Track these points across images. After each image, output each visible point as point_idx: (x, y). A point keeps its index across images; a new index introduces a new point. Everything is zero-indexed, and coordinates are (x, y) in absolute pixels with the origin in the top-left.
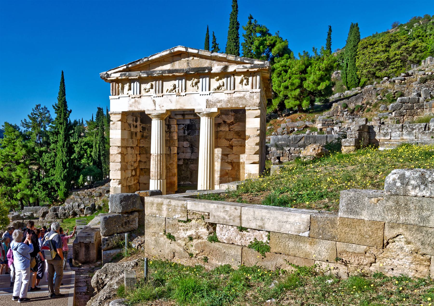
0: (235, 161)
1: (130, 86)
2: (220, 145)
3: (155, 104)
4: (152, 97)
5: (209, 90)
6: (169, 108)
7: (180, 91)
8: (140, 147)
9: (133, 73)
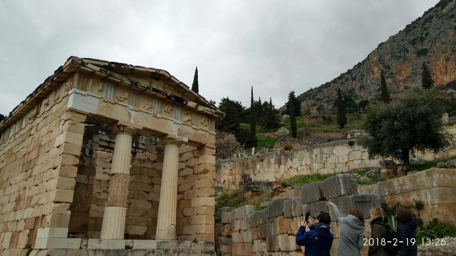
0: (155, 199)
3: (130, 117)
4: (128, 108)
7: (156, 113)
9: (116, 75)
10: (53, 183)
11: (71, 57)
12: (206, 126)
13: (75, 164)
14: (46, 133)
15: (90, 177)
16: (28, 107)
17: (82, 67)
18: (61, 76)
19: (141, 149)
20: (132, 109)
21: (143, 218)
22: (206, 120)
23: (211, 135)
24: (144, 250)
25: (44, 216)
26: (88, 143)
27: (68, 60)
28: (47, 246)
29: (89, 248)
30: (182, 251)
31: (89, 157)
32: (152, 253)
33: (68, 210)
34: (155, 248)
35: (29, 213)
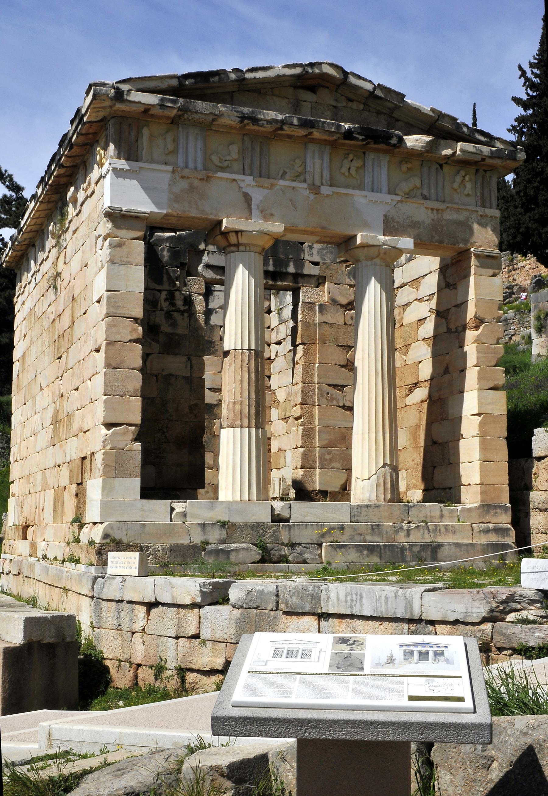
1: (175, 140)
2: (324, 362)
7: (317, 183)
9: (200, 105)
10: (97, 385)
11: (90, 86)
13: (135, 336)
14: (79, 269)
15: (195, 360)
16: (44, 206)
18: (83, 132)
19: (310, 276)
21: (334, 451)
22: (467, 178)
25: (93, 454)
27: (87, 93)
28: (101, 515)
29: (188, 519)
30: (417, 527)
31: (184, 311)
33: (136, 440)
34: (345, 519)
35: (73, 449)
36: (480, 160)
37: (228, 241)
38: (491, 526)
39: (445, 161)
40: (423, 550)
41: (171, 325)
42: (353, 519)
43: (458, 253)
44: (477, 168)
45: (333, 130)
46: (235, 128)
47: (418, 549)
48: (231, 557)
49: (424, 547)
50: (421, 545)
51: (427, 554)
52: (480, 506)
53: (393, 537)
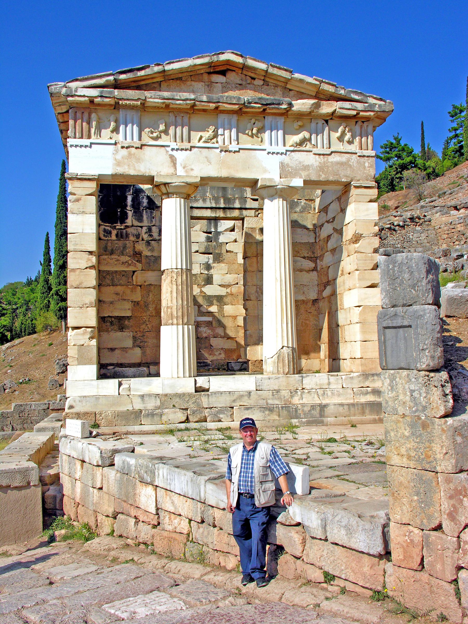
5: (284, 145)
6: (205, 175)
7: (227, 142)
8: (99, 270)
12: (350, 142)
17: (70, 99)
20: (176, 147)
23: (362, 159)
24: (230, 392)
26: (153, 218)
29: (132, 393)
32: (246, 398)
33: (92, 338)
36: (355, 114)
37: (161, 192)
38: (369, 389)
39: (330, 118)
40: (313, 409)
41: (150, 250)
42: (258, 388)
43: (345, 186)
44: (356, 120)
45: (234, 102)
46: (162, 108)
47: (310, 409)
48: (163, 418)
49: (313, 407)
50: (311, 406)
51: (316, 413)
52: (360, 375)
53: (290, 400)
